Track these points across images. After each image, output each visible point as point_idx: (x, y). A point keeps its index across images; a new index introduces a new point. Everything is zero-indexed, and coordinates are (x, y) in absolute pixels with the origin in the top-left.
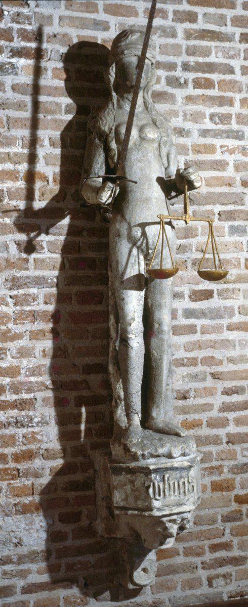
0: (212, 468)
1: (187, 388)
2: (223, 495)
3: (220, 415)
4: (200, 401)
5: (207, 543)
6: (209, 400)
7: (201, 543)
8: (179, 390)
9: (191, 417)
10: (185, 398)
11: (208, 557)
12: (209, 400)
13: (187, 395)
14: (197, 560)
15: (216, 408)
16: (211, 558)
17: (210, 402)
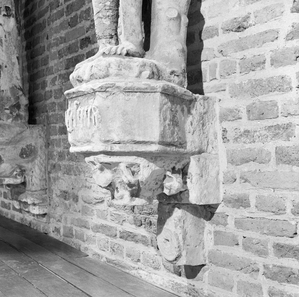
0: (278, 127)
1: (244, 14)
2: (292, 171)
3: (287, 46)
4: (261, 28)
5: (273, 240)
6: (273, 25)
7: (264, 238)
8: (235, 19)
9: (249, 53)
10: (240, 28)
11: (273, 260)
12: (273, 25)
13: (245, 23)
14: (260, 261)
15: (282, 35)
16: (275, 264)
17: (275, 27)
